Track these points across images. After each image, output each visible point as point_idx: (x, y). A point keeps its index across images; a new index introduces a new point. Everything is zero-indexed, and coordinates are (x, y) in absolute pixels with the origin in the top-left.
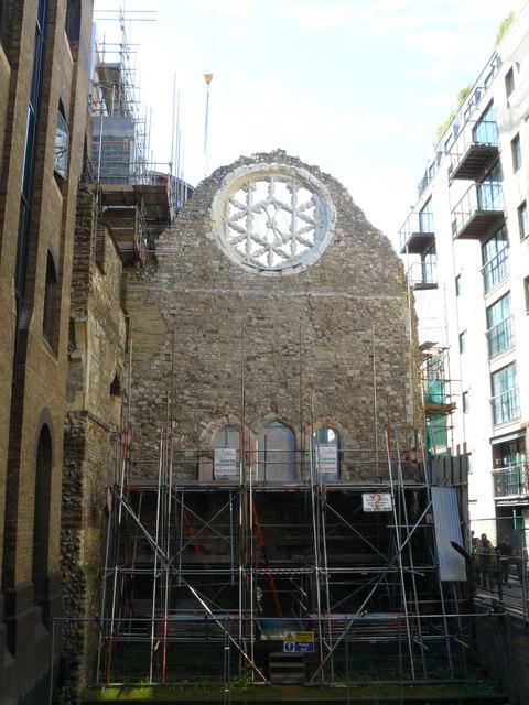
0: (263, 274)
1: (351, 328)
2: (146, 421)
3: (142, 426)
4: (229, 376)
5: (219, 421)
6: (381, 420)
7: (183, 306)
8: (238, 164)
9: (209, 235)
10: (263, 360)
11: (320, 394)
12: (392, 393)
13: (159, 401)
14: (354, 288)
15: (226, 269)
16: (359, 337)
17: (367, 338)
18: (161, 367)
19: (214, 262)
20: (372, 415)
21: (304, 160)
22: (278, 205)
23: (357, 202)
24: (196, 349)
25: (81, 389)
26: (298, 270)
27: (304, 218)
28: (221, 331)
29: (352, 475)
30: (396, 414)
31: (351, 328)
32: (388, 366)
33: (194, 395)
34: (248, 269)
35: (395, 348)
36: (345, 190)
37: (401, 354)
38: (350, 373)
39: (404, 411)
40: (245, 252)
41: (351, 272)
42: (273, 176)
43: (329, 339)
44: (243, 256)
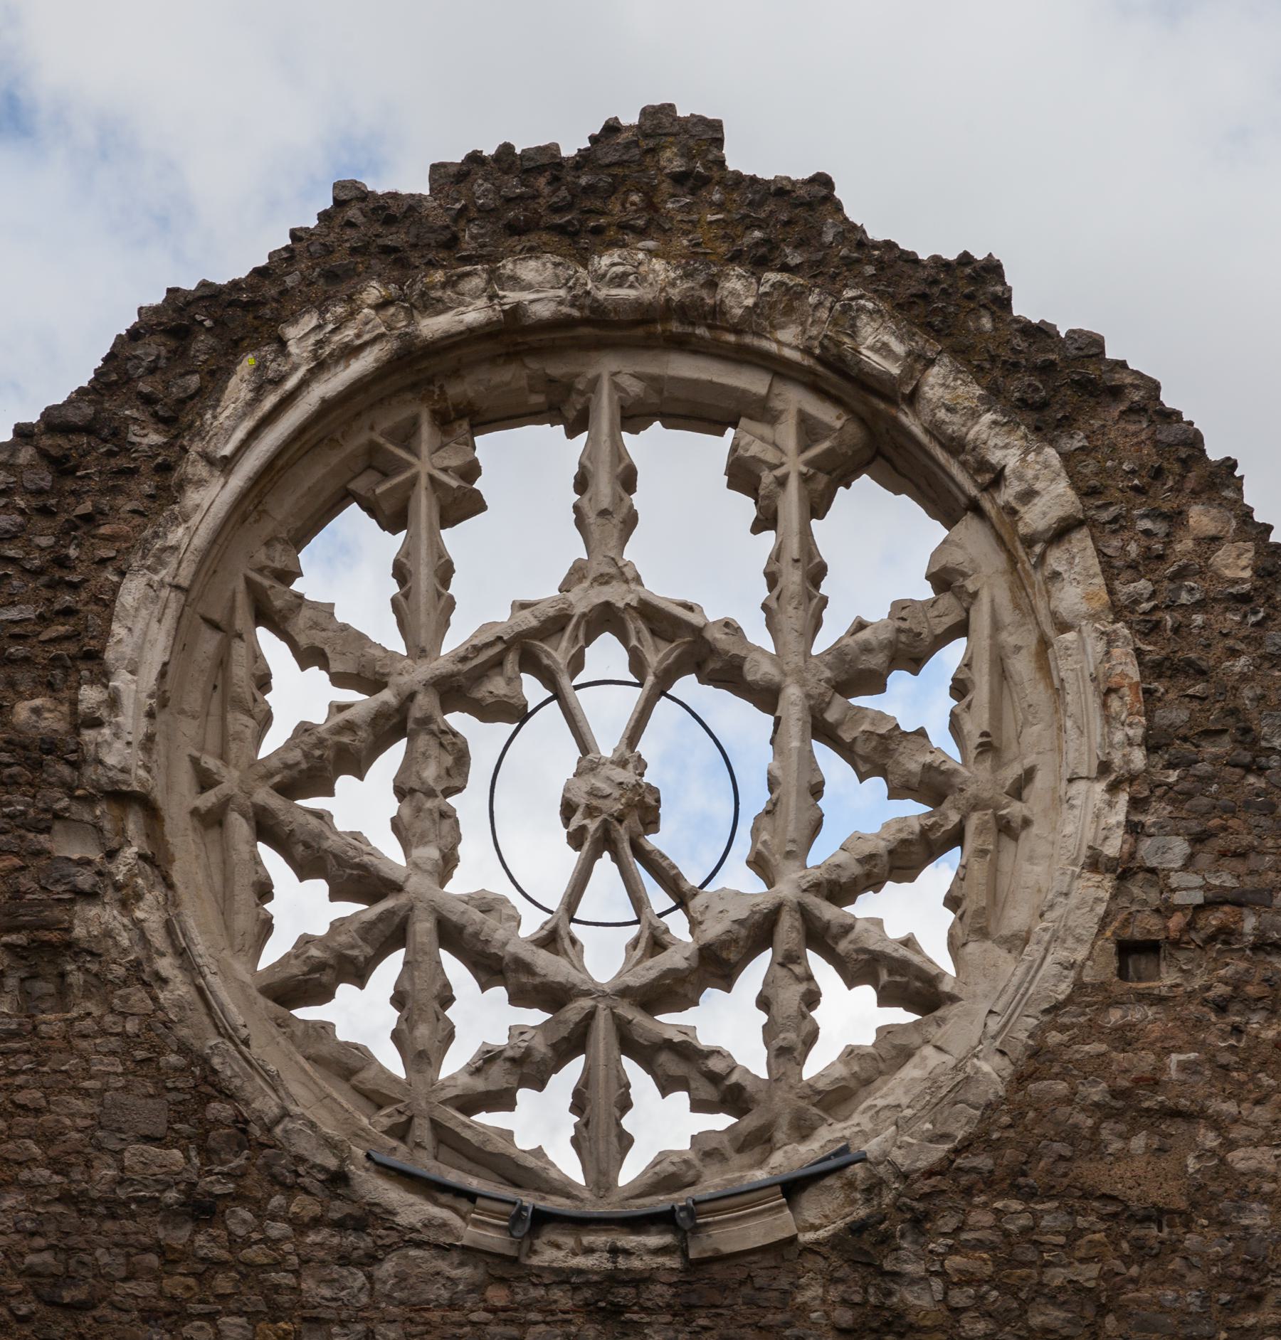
19: (134, 1154)
40: (391, 1060)
41: (1257, 1218)
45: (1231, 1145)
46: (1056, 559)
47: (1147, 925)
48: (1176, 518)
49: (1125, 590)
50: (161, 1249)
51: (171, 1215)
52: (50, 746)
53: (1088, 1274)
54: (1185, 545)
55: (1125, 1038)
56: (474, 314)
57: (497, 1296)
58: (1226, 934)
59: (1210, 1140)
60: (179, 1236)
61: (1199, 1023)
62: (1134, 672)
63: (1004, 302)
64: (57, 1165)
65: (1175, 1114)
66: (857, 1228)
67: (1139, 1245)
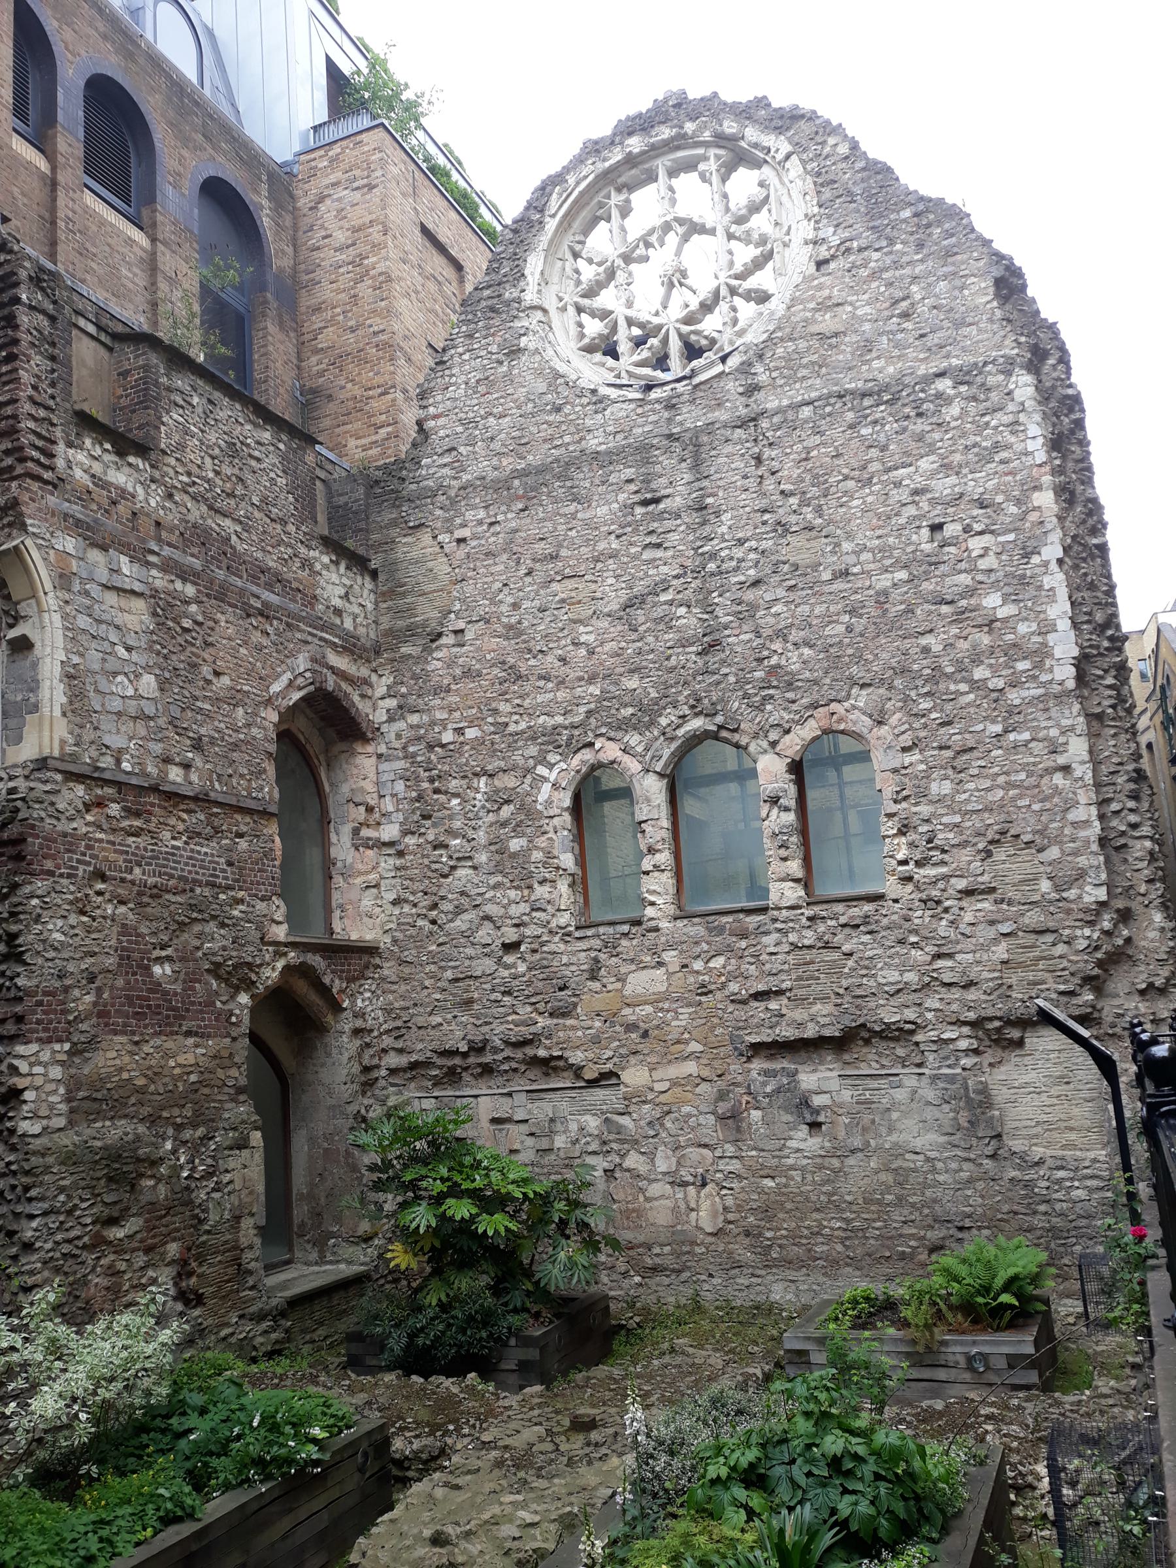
0: (655, 394)
1: (875, 467)
2: (426, 785)
3: (419, 798)
4: (591, 653)
5: (576, 761)
6: (976, 686)
7: (482, 514)
8: (579, 161)
9: (523, 341)
10: (664, 597)
11: (806, 651)
12: (1000, 614)
13: (448, 737)
14: (876, 364)
15: (567, 409)
16: (898, 484)
17: (919, 481)
18: (450, 663)
20: (948, 676)
21: (728, 96)
22: (694, 228)
23: (874, 149)
24: (515, 606)
25: (35, 708)
26: (733, 362)
27: (747, 239)
28: (564, 553)
29: (912, 845)
30: (1022, 666)
31: (875, 467)
32: (987, 540)
33: (521, 711)
34: (613, 393)
35: (997, 490)
36: (838, 130)
37: (1018, 502)
38: (884, 582)
39: (1041, 655)
41: (867, 327)
42: (661, 165)
43: (819, 511)
44: (611, 370)
45: (856, 308)
46: (787, 165)
47: (824, 253)
48: (824, 143)
49: (809, 167)
50: (546, 422)
51: (550, 412)
52: (513, 300)
53: (815, 358)
54: (827, 149)
55: (820, 287)
56: (619, 157)
57: (640, 411)
58: (848, 250)
59: (849, 309)
60: (551, 418)
61: (843, 277)
62: (812, 186)
63: (769, 105)
64: (519, 408)
65: (838, 305)
66: (742, 363)
67: (830, 345)
